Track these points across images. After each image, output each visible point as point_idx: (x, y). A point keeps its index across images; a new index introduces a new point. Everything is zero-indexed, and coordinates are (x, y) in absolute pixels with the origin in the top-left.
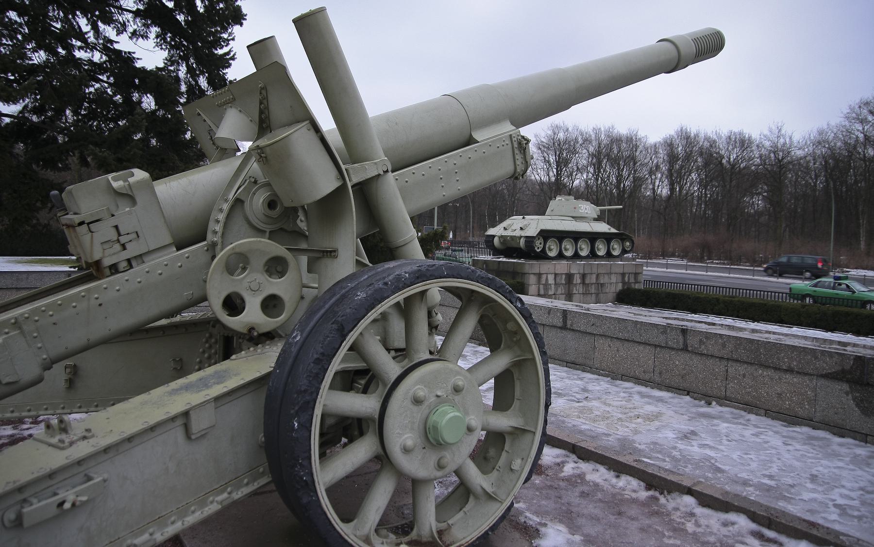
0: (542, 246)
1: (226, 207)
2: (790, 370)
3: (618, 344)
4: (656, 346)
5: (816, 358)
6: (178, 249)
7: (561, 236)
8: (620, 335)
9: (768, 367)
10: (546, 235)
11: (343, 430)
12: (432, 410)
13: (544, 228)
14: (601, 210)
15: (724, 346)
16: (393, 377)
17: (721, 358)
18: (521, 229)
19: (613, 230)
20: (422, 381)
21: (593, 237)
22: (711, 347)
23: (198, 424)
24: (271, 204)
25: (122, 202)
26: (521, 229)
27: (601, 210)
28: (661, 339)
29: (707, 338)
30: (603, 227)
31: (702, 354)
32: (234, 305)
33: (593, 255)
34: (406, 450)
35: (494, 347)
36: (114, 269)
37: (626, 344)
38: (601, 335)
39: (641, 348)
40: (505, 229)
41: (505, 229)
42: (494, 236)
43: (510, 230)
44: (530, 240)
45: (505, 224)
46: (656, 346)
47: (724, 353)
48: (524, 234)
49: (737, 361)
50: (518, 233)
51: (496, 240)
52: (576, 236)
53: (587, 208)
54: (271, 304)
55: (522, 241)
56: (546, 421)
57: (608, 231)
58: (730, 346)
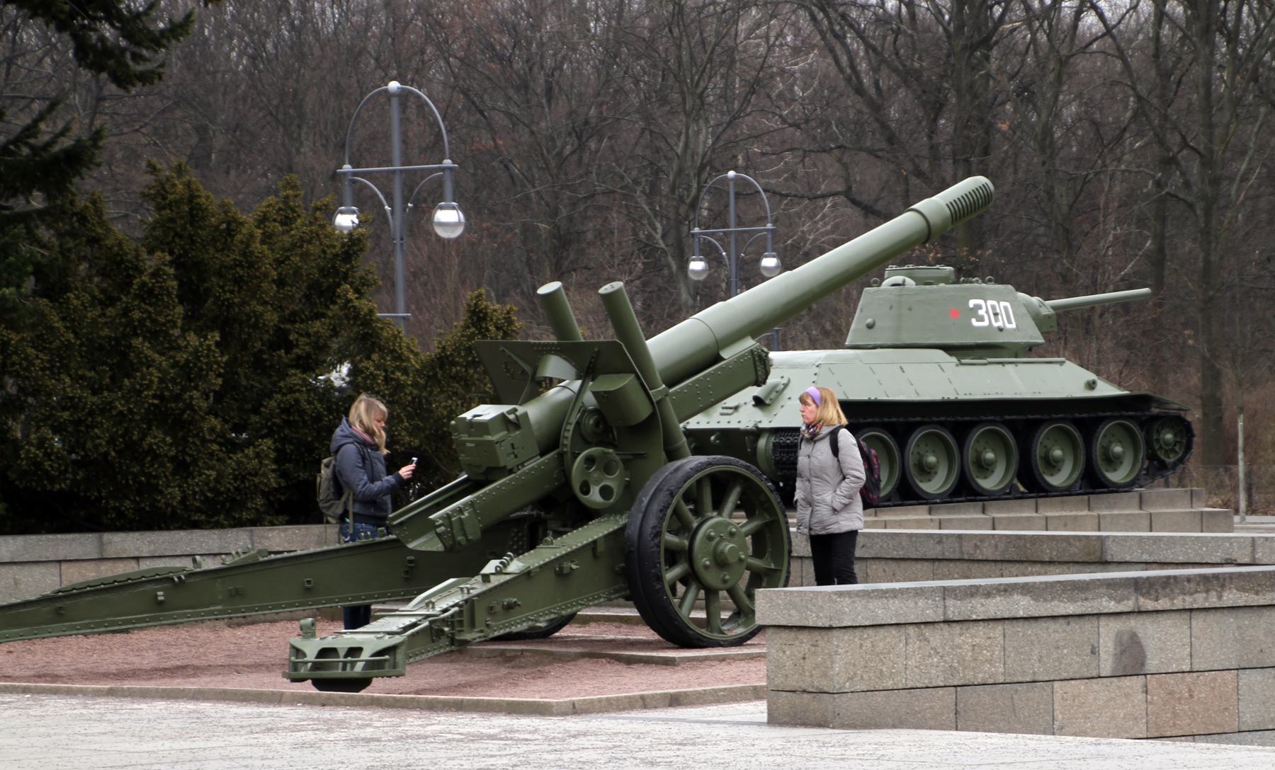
1: (571, 428)
6: (542, 455)
8: (895, 554)
9: (1035, 562)
11: (673, 556)
12: (718, 544)
14: (1062, 312)
16: (695, 525)
19: (1106, 390)
20: (712, 527)
22: (988, 553)
23: (601, 548)
24: (597, 424)
25: (511, 428)
28: (935, 551)
29: (981, 541)
30: (1064, 380)
32: (586, 489)
34: (706, 567)
35: (750, 515)
36: (511, 472)
37: (903, 564)
38: (873, 558)
39: (919, 565)
46: (933, 560)
54: (606, 492)
56: (789, 572)
57: (1080, 392)
58: (1001, 546)
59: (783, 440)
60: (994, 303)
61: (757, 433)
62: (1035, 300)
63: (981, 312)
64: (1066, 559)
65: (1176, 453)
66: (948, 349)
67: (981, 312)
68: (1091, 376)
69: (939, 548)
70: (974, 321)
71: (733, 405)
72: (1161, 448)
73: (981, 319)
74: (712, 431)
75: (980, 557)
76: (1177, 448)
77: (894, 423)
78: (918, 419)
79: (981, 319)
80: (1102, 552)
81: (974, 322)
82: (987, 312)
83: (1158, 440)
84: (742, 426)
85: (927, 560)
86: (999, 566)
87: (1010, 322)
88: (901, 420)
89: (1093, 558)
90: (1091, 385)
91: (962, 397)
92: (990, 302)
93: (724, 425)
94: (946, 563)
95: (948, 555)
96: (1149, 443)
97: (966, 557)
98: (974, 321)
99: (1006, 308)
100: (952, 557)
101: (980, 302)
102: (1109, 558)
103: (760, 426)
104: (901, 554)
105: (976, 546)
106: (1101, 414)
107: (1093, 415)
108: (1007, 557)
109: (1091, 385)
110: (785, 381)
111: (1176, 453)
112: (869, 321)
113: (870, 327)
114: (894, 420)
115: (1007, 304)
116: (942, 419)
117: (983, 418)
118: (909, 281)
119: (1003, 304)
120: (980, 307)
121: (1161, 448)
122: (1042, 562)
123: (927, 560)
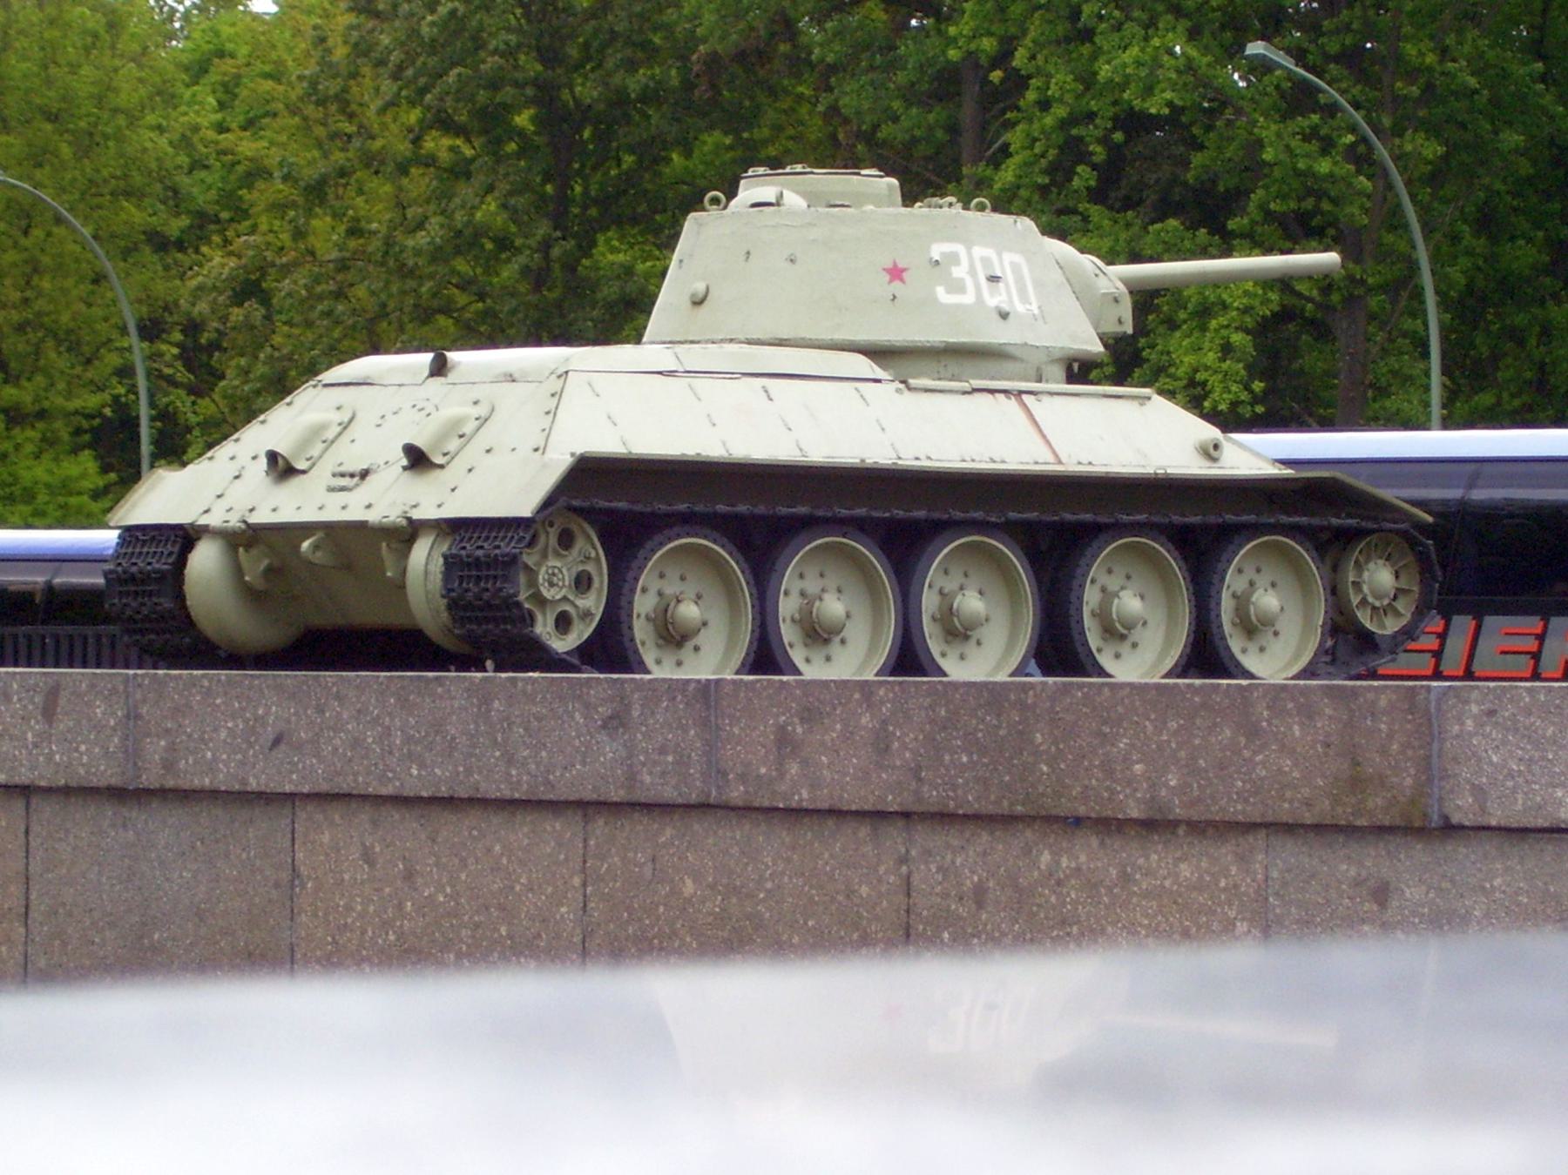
0: (594, 602)
2: (1155, 826)
3: (407, 830)
4: (587, 808)
5: (1253, 732)
7: (758, 514)
8: (414, 780)
10: (620, 504)
13: (608, 443)
15: (881, 744)
17: (878, 816)
18: (417, 459)
21: (1054, 526)
26: (417, 459)
27: (1146, 299)
30: (1151, 436)
31: (796, 814)
37: (455, 829)
39: (521, 832)
40: (281, 468)
41: (281, 468)
42: (185, 537)
43: (321, 477)
44: (481, 548)
45: (279, 427)
46: (587, 808)
47: (885, 792)
48: (434, 499)
49: (944, 818)
50: (387, 499)
51: (205, 560)
52: (900, 517)
53: (1016, 276)
55: (424, 557)
57: (1190, 466)
59: (476, 549)
60: (990, 253)
61: (410, 531)
62: (1089, 262)
63: (959, 272)
64: (1238, 810)
65: (1398, 614)
66: (879, 353)
67: (959, 272)
68: (1211, 432)
69: (610, 750)
70: (940, 291)
71: (358, 467)
72: (1364, 602)
73: (957, 287)
74: (306, 529)
75: (803, 797)
76: (1400, 605)
77: (737, 517)
78: (802, 510)
79: (957, 287)
80: (1430, 772)
82: (972, 272)
83: (1357, 585)
84: (373, 517)
85: (555, 807)
86: (894, 838)
87: (1025, 299)
88: (761, 509)
89: (1377, 806)
90: (1210, 452)
91: (908, 462)
92: (978, 251)
93: (333, 514)
94: (641, 825)
95: (652, 785)
96: (1334, 591)
97: (736, 794)
98: (940, 291)
99: (1016, 268)
100: (669, 794)
101: (960, 248)
102: (1462, 808)
103: (416, 515)
104: (438, 776)
105: (784, 742)
106: (1230, 518)
107: (1212, 519)
108: (932, 797)
109: (1210, 452)
110: (481, 411)
111: (1398, 614)
112: (700, 287)
113: (698, 302)
114: (742, 508)
115: (1018, 258)
116: (861, 512)
117: (958, 515)
118: (793, 200)
119: (1008, 257)
120: (954, 259)
121: (1364, 602)
122: (1109, 826)
123: (555, 807)
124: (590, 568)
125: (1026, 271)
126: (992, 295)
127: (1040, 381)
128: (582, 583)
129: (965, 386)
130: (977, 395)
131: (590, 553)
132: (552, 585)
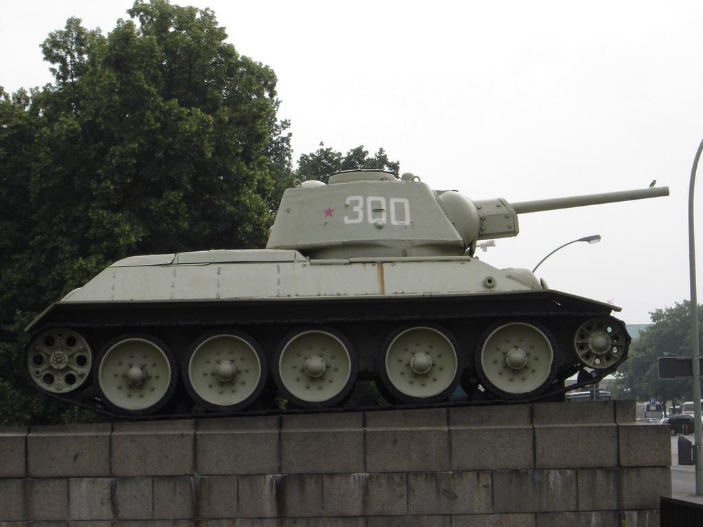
33: (370, 394)
63: (356, 209)
67: (356, 209)
73: (356, 216)
81: (347, 220)
82: (365, 208)
98: (346, 218)
101: (361, 199)
120: (356, 203)
124: (84, 354)
125: (407, 207)
126: (374, 217)
127: (406, 256)
128: (82, 361)
129: (347, 261)
130: (353, 265)
131: (83, 347)
132: (58, 363)
